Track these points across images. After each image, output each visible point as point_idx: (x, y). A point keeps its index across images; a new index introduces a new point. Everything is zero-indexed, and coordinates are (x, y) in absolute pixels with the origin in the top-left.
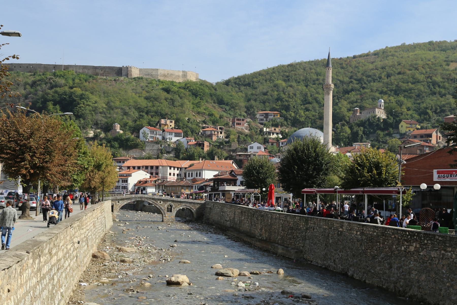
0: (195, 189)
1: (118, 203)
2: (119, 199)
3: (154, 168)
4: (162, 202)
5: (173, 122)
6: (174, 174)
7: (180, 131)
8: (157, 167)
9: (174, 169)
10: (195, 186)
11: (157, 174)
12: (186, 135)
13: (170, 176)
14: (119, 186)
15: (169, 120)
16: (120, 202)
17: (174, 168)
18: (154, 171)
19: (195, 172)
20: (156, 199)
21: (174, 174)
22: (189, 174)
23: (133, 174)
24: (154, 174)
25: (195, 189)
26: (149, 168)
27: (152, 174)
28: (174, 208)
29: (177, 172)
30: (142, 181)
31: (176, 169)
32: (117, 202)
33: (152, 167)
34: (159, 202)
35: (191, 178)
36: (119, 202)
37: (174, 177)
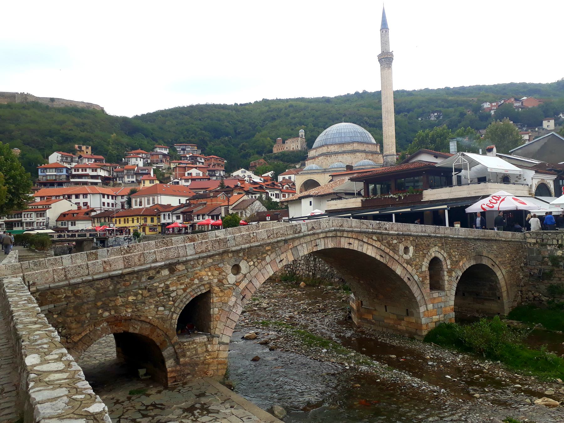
0: (164, 219)
1: (232, 278)
3: (81, 196)
4: (411, 249)
5: (90, 148)
6: (108, 204)
7: (101, 157)
9: (108, 198)
10: (164, 215)
13: (104, 207)
14: (33, 222)
15: (85, 147)
16: (244, 266)
17: (108, 196)
19: (146, 199)
21: (108, 204)
22: (136, 201)
24: (81, 205)
25: (164, 219)
26: (74, 197)
28: (450, 271)
29: (110, 201)
30: (67, 214)
31: (110, 197)
32: (228, 268)
34: (401, 247)
35: (138, 207)
37: (113, 208)
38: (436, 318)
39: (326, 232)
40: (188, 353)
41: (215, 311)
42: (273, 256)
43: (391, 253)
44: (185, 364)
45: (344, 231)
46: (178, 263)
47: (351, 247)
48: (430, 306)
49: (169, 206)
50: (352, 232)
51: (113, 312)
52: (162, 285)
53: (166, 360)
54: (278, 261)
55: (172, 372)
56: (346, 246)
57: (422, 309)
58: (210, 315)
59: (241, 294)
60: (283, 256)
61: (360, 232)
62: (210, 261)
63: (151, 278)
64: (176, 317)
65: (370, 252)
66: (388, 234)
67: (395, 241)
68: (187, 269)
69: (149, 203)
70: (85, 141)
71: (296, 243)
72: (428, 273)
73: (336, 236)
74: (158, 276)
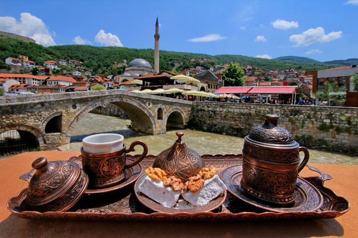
1: (72, 110)
2: (74, 100)
7: (33, 62)
8: (24, 78)
11: (24, 82)
12: (37, 64)
16: (78, 105)
18: (22, 80)
20: (144, 99)
23: (6, 81)
24: (22, 82)
26: (18, 79)
27: (20, 82)
28: (165, 113)
33: (20, 78)
36: (74, 107)
38: (159, 129)
39: (117, 95)
40: (51, 140)
41: (64, 123)
42: (93, 102)
43: (143, 105)
44: (49, 144)
45: (124, 95)
46: (45, 102)
47: (127, 102)
48: (157, 125)
49: (64, 86)
50: (128, 95)
51: (11, 121)
52: (38, 111)
53: (39, 142)
54: (94, 105)
55: (43, 147)
56: (125, 101)
57: (154, 126)
58: (61, 125)
59: (77, 117)
60: (97, 103)
61: (131, 96)
62: (61, 102)
63: (32, 108)
64: (45, 124)
65: (135, 104)
66: (142, 98)
67: (145, 101)
68: (50, 105)
69: (55, 83)
70: (25, 54)
71: (103, 98)
72: (157, 113)
73: (121, 97)
74: (35, 107)
